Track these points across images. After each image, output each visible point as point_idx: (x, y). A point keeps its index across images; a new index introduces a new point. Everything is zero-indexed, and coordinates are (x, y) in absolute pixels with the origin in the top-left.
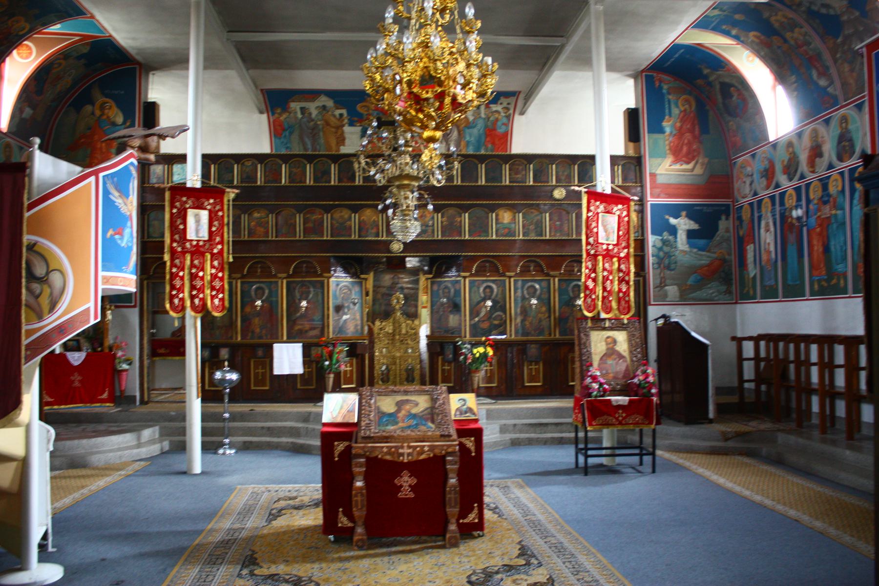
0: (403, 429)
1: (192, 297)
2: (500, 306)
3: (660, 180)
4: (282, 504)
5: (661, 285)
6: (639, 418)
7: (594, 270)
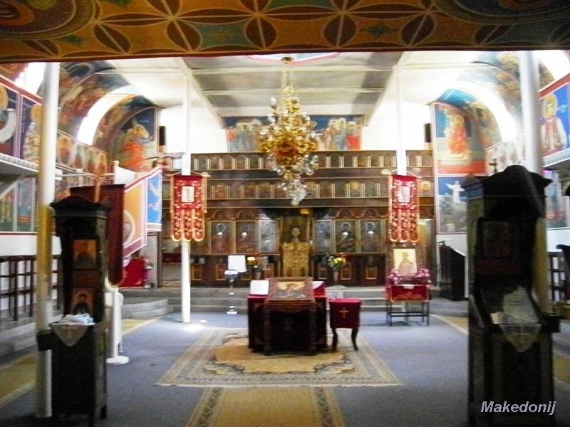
0: (288, 298)
1: (186, 231)
2: (352, 235)
3: (444, 163)
4: (230, 336)
5: (443, 224)
6: (419, 296)
7: (396, 217)
